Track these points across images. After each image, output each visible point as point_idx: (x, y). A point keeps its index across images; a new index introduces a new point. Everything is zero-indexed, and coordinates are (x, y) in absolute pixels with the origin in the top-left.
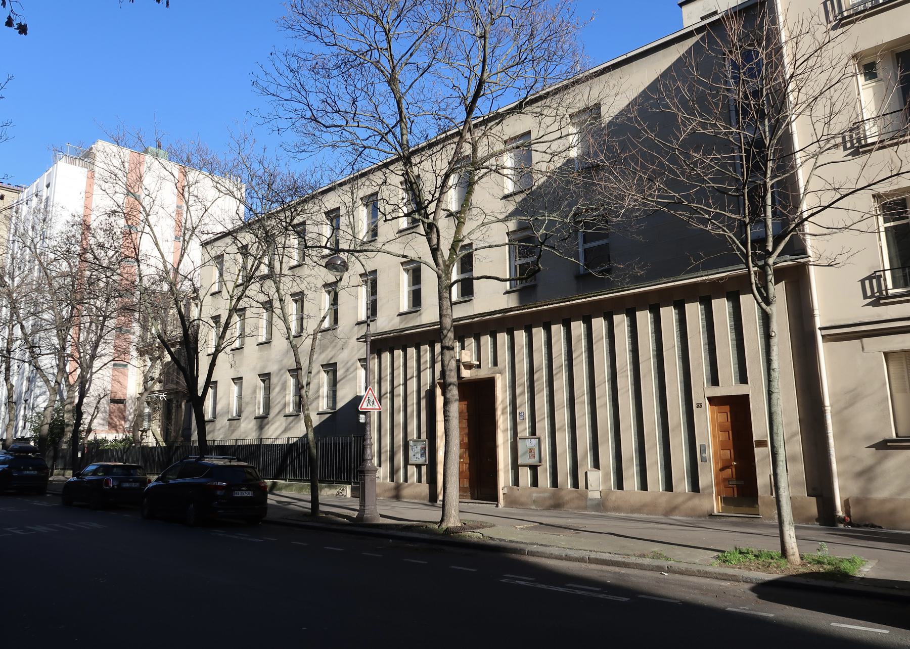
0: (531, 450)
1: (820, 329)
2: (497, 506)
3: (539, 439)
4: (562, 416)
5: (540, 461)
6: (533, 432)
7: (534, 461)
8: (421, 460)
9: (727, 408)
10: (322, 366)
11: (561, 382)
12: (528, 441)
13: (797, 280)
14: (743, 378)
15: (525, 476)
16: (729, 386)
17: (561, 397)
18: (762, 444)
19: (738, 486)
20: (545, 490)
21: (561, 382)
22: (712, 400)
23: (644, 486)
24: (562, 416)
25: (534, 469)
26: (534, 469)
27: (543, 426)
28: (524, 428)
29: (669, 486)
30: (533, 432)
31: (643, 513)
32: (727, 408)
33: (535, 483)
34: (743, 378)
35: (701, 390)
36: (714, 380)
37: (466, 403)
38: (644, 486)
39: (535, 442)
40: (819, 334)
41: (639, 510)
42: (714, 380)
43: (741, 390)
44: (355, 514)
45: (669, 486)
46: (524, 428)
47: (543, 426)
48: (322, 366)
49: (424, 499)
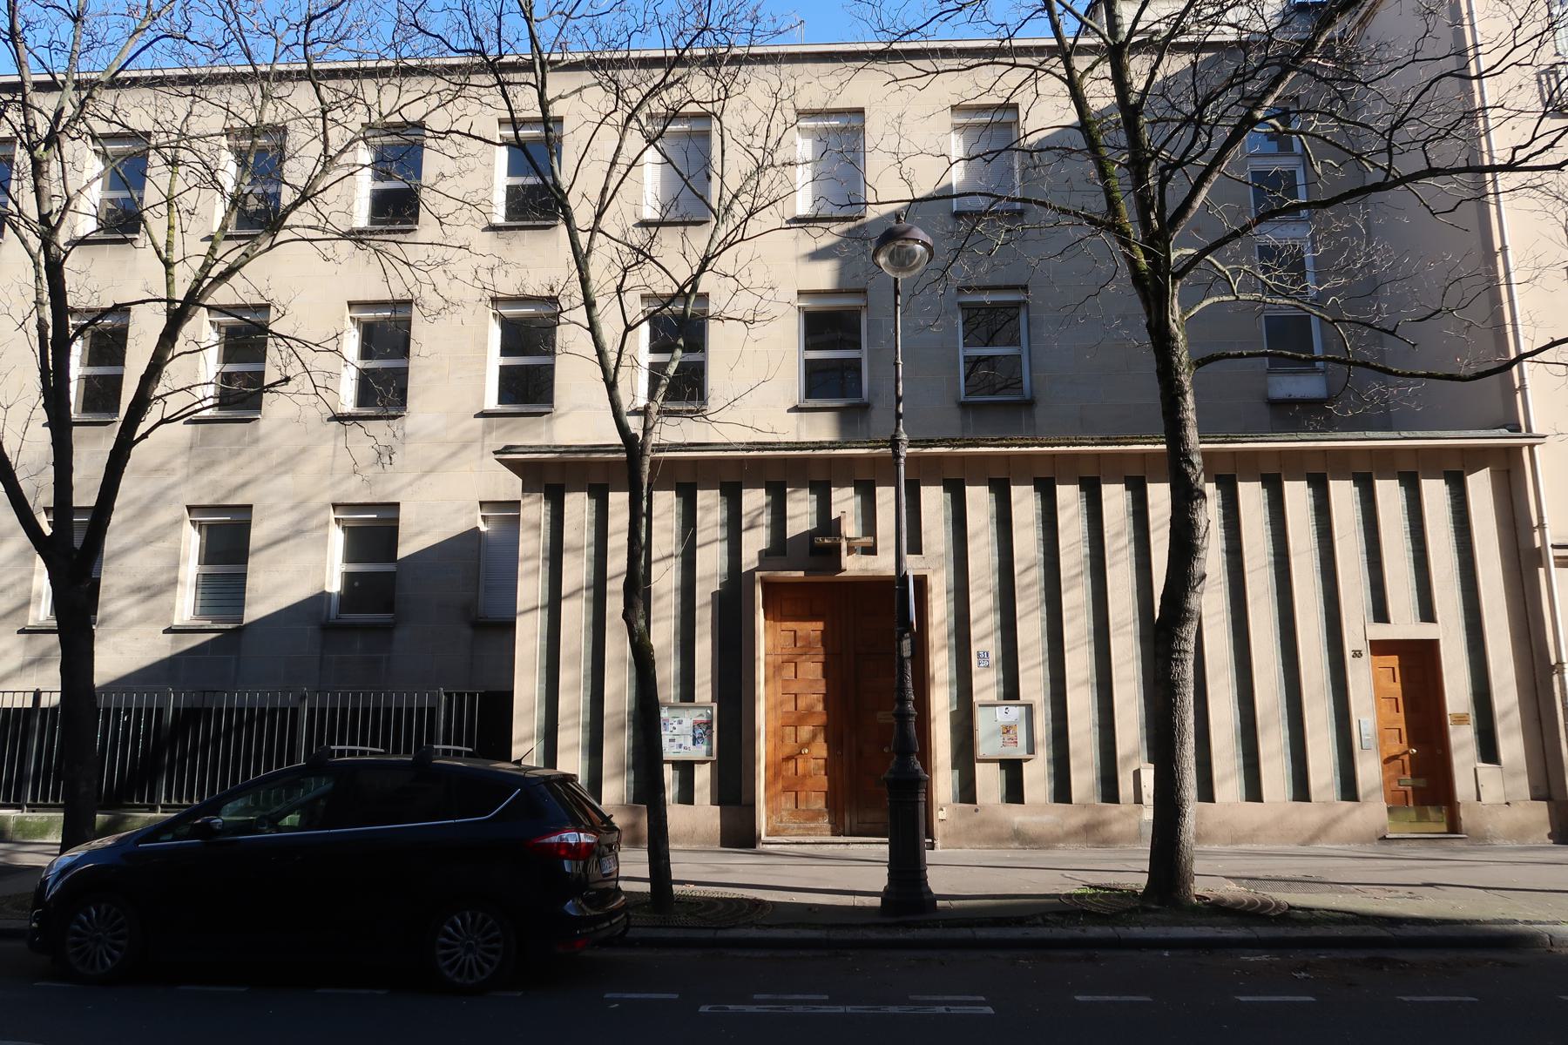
0: (1007, 729)
1: (1554, 546)
3: (1029, 708)
4: (1080, 663)
5: (1031, 749)
6: (1011, 690)
7: (1019, 752)
8: (699, 752)
9: (1394, 661)
10: (190, 508)
11: (1075, 598)
12: (1000, 711)
13: (1510, 470)
14: (1427, 613)
15: (989, 779)
16: (1404, 625)
17: (1077, 627)
18: (1461, 720)
19: (1414, 789)
21: (1075, 598)
22: (1380, 648)
23: (1254, 791)
24: (1080, 663)
25: (1013, 770)
26: (1013, 770)
27: (1034, 682)
28: (986, 682)
29: (1301, 790)
30: (1011, 690)
31: (1258, 843)
32: (1394, 661)
33: (1014, 793)
34: (1427, 613)
35: (1358, 628)
36: (1381, 613)
38: (1254, 791)
39: (1015, 713)
40: (1551, 553)
41: (1251, 836)
42: (1381, 613)
43: (1424, 632)
44: (877, 902)
45: (1301, 790)
46: (986, 682)
47: (1034, 682)
48: (190, 508)
49: (712, 843)
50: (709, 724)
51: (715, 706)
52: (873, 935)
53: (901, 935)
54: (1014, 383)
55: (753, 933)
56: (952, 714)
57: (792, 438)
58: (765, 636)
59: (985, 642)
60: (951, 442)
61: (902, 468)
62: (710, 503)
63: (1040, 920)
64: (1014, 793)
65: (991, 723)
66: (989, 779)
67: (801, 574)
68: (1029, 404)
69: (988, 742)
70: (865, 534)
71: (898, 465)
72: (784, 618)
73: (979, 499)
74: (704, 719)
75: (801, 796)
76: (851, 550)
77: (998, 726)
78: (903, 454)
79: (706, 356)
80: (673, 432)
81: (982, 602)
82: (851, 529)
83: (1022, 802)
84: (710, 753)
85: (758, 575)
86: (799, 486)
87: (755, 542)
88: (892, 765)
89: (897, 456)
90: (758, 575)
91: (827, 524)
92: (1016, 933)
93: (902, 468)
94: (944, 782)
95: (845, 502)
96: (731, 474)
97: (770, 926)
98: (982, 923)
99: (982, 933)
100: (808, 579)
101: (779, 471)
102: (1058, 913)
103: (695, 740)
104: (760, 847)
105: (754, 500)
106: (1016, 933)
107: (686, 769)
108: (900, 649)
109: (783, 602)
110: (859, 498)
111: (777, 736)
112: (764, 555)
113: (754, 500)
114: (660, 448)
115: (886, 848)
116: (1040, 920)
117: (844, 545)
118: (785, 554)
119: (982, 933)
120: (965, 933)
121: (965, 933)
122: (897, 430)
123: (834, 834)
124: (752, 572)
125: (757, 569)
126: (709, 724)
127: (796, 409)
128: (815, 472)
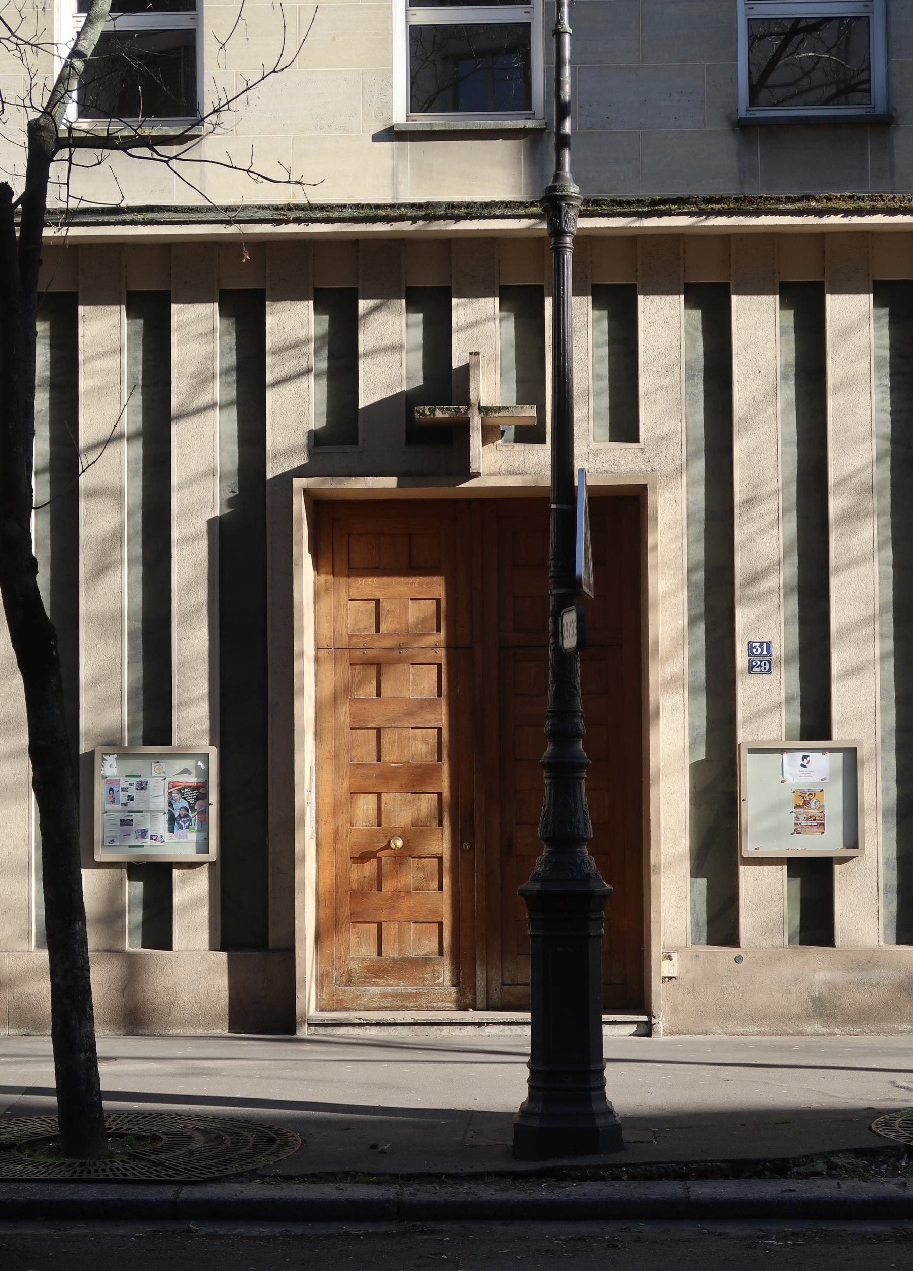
0: (804, 799)
2: (647, 1030)
3: (851, 755)
5: (853, 840)
6: (815, 722)
7: (824, 843)
12: (791, 761)
15: (765, 896)
20: (866, 961)
25: (814, 880)
26: (814, 880)
28: (765, 702)
30: (815, 722)
37: (437, 587)
46: (765, 702)
49: (211, 1024)
50: (201, 791)
51: (213, 752)
52: (488, 1193)
53: (543, 1193)
54: (852, 85)
55: (254, 1191)
56: (697, 769)
57: (383, 197)
58: (317, 606)
59: (764, 621)
60: (707, 205)
61: (568, 256)
62: (198, 332)
63: (820, 1166)
64: (816, 923)
65: (780, 788)
66: (765, 896)
67: (390, 482)
68: (883, 123)
69: (765, 824)
70: (522, 400)
71: (559, 250)
72: (354, 571)
73: (759, 326)
74: (192, 780)
75: (390, 931)
76: (490, 434)
77: (787, 794)
78: (569, 228)
79: (198, 19)
80: (100, 183)
81: (764, 539)
82: (491, 387)
83: (834, 946)
84: (203, 848)
85: (299, 483)
86: (384, 293)
87: (295, 410)
88: (538, 867)
89: (557, 232)
90: (299, 483)
91: (444, 379)
92: (769, 1189)
93: (568, 256)
94: (674, 899)
95: (481, 328)
96: (244, 269)
97: (289, 1178)
98: (706, 1173)
99: (703, 1190)
100: (401, 490)
101: (349, 265)
102: (859, 1153)
103: (172, 821)
104: (304, 1032)
105: (293, 323)
106: (769, 1189)
107: (156, 877)
108: (557, 633)
109: (352, 538)
110: (510, 326)
111: (336, 810)
112: (317, 440)
113: (293, 323)
114: (72, 216)
115: (527, 1030)
116: (820, 1166)
117: (476, 421)
118: (355, 442)
119: (703, 1190)
120: (672, 1189)
121: (672, 1189)
122: (558, 176)
123: (463, 1008)
124: (286, 479)
125: (300, 472)
126: (201, 791)
127: (392, 134)
128: (419, 263)
